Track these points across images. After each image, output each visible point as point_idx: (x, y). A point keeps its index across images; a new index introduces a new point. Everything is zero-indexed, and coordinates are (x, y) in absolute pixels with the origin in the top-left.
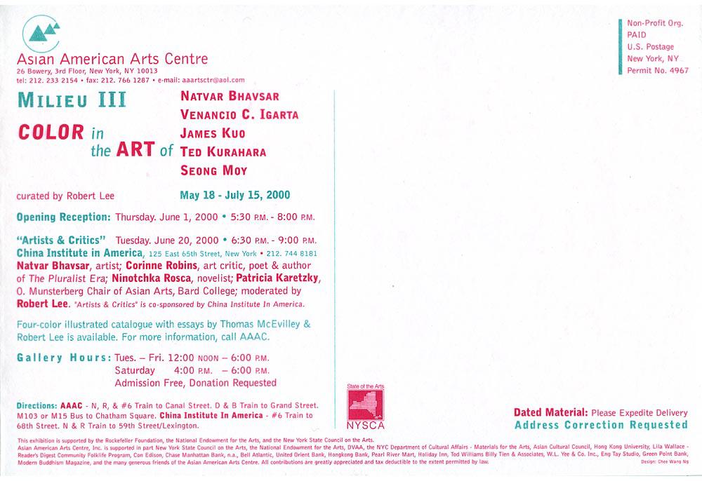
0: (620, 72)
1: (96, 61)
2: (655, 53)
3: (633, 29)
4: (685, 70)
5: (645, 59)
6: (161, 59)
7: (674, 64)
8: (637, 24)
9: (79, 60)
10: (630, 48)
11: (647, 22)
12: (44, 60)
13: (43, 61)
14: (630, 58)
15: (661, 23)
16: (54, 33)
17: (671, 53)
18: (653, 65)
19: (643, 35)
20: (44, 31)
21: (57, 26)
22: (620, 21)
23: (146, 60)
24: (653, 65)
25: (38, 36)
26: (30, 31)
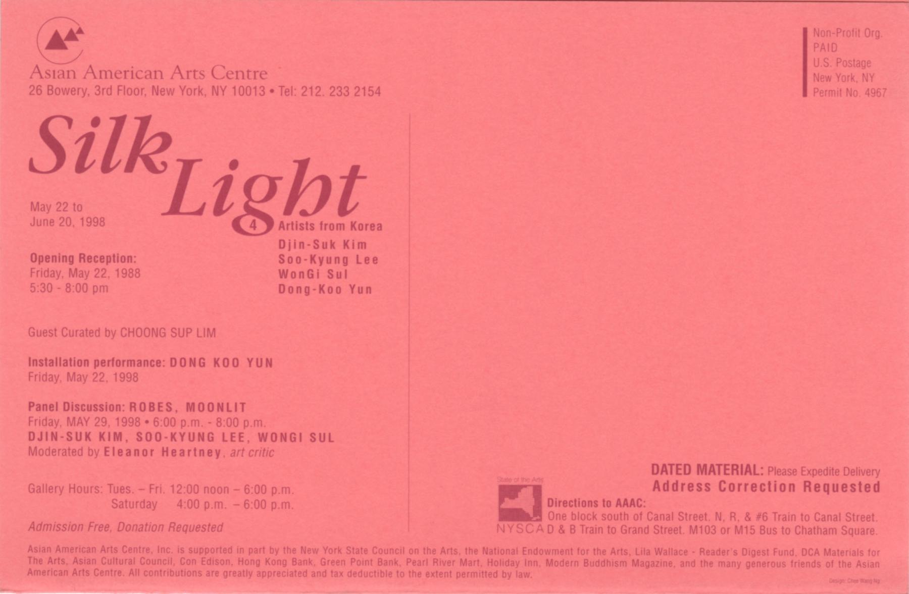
0: (805, 94)
1: (129, 75)
2: (846, 71)
3: (820, 40)
4: (882, 91)
5: (834, 79)
7: (869, 85)
8: (828, 33)
9: (109, 73)
10: (816, 64)
11: (839, 31)
12: (63, 74)
13: (65, 75)
14: (817, 78)
15: (855, 32)
16: (76, 39)
17: (867, 70)
18: (844, 86)
19: (833, 47)
20: (63, 35)
21: (80, 31)
22: (805, 31)
23: (191, 75)
24: (844, 86)
25: (56, 43)
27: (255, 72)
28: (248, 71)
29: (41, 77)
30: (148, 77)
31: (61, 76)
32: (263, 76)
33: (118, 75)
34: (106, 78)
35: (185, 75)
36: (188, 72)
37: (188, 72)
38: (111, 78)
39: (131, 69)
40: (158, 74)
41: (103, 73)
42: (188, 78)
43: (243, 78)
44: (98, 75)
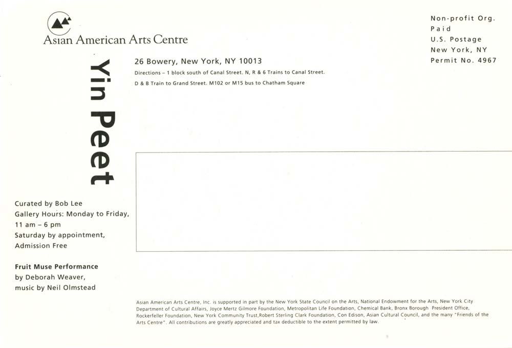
1: (104, 41)
6: (152, 40)
9: (92, 41)
12: (64, 41)
16: (68, 24)
20: (61, 22)
23: (142, 41)
25: (57, 25)
26: (52, 23)
27: (180, 39)
28: (176, 38)
29: (51, 43)
30: (116, 42)
31: (63, 43)
32: (185, 41)
33: (97, 42)
34: (90, 43)
35: (138, 41)
36: (140, 39)
37: (140, 39)
38: (93, 43)
39: (105, 38)
40: (123, 41)
41: (88, 40)
42: (140, 43)
43: (173, 43)
44: (85, 42)
